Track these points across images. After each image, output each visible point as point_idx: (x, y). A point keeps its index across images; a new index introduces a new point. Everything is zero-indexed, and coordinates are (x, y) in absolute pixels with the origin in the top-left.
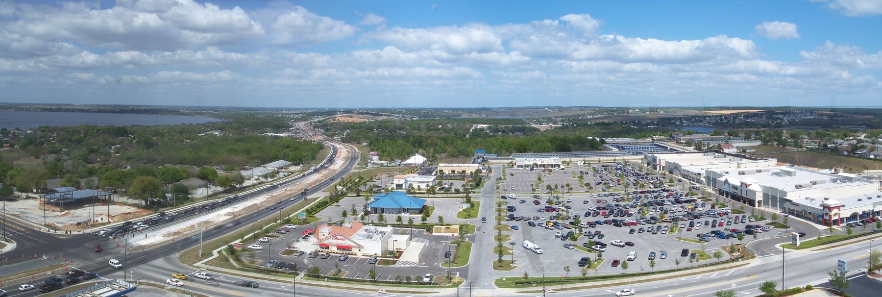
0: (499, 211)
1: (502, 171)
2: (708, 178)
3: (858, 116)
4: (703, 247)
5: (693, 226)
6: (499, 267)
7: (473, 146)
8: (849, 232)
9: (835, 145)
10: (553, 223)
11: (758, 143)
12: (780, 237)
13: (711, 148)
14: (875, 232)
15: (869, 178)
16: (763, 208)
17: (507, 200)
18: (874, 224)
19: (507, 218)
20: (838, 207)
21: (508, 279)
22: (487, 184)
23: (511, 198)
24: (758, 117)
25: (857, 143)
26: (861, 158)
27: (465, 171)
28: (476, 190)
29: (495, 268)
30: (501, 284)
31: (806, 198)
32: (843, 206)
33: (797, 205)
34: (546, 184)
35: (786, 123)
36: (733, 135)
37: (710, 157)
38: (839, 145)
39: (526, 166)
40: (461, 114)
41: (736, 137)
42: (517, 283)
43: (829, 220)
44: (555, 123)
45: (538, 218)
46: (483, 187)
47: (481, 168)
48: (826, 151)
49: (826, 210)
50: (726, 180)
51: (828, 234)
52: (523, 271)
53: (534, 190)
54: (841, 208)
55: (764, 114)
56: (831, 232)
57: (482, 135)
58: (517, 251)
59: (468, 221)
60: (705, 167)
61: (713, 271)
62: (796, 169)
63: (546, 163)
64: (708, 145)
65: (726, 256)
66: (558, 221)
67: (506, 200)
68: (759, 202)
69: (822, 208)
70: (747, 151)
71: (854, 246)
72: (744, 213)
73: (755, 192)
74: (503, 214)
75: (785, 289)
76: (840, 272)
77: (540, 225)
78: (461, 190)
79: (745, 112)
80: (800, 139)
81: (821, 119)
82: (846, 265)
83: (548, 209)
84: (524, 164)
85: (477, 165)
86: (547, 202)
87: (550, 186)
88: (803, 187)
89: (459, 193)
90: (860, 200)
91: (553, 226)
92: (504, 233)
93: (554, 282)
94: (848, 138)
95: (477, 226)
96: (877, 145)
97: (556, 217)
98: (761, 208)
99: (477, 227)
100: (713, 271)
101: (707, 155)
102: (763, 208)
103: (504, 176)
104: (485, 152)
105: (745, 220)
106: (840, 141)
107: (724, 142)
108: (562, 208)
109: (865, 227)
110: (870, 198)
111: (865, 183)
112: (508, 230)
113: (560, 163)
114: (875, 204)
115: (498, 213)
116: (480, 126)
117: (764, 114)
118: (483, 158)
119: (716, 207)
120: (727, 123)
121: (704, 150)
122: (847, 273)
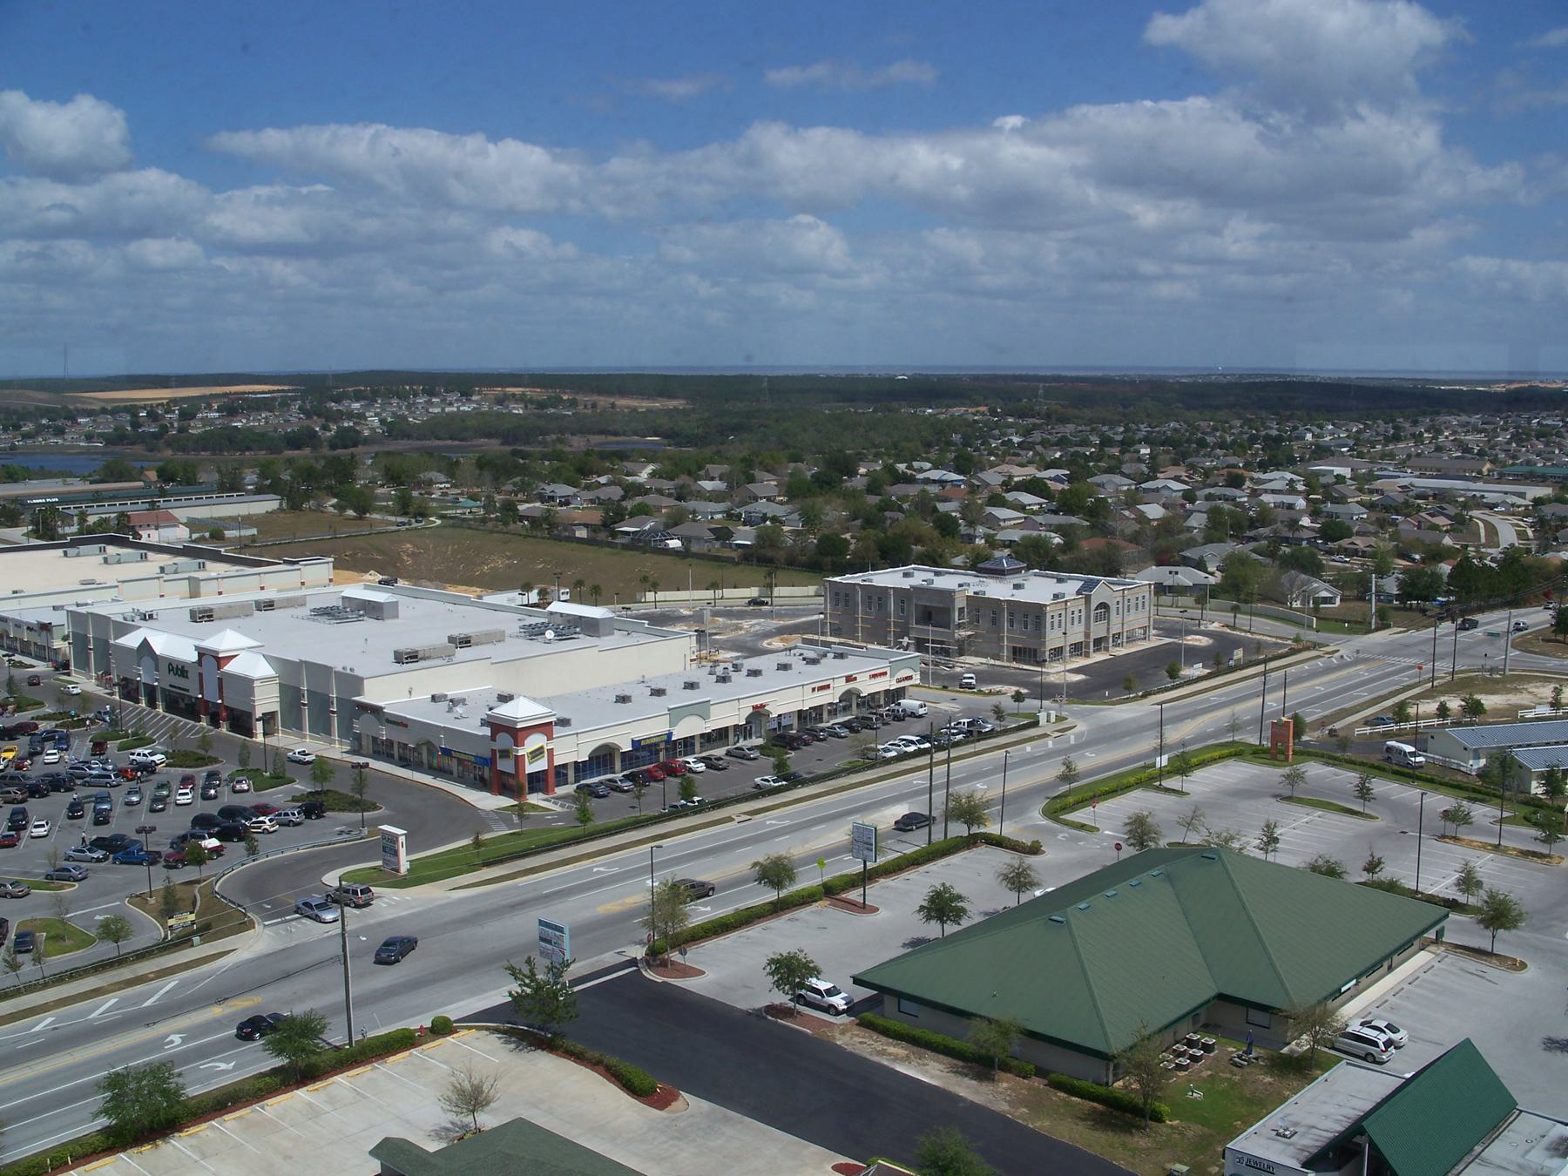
2: (80, 642)
4: (59, 902)
5: (24, 828)
11: (269, 504)
12: (340, 842)
13: (90, 530)
14: (677, 813)
15: (661, 621)
18: (674, 782)
20: (545, 728)
25: (624, 498)
26: (636, 548)
31: (434, 698)
32: (564, 722)
33: (400, 723)
35: (373, 429)
37: (88, 563)
38: (561, 504)
41: (189, 484)
43: (515, 776)
48: (512, 526)
49: (504, 740)
50: (145, 643)
51: (510, 825)
54: (558, 732)
56: (521, 817)
60: (69, 601)
61: (97, 992)
62: (403, 592)
64: (83, 517)
65: (151, 929)
68: (268, 718)
69: (487, 731)
70: (229, 534)
71: (599, 867)
72: (216, 760)
73: (252, 681)
75: (357, 1037)
76: (547, 962)
79: (225, 395)
80: (418, 485)
81: (499, 415)
82: (566, 937)
88: (423, 659)
90: (623, 699)
94: (595, 478)
96: (692, 504)
98: (271, 741)
100: (97, 992)
101: (78, 555)
102: (283, 740)
105: (215, 787)
106: (563, 490)
107: (141, 505)
109: (638, 797)
110: (658, 692)
114: (676, 714)
117: (294, 399)
119: (112, 745)
121: (64, 536)
122: (568, 966)
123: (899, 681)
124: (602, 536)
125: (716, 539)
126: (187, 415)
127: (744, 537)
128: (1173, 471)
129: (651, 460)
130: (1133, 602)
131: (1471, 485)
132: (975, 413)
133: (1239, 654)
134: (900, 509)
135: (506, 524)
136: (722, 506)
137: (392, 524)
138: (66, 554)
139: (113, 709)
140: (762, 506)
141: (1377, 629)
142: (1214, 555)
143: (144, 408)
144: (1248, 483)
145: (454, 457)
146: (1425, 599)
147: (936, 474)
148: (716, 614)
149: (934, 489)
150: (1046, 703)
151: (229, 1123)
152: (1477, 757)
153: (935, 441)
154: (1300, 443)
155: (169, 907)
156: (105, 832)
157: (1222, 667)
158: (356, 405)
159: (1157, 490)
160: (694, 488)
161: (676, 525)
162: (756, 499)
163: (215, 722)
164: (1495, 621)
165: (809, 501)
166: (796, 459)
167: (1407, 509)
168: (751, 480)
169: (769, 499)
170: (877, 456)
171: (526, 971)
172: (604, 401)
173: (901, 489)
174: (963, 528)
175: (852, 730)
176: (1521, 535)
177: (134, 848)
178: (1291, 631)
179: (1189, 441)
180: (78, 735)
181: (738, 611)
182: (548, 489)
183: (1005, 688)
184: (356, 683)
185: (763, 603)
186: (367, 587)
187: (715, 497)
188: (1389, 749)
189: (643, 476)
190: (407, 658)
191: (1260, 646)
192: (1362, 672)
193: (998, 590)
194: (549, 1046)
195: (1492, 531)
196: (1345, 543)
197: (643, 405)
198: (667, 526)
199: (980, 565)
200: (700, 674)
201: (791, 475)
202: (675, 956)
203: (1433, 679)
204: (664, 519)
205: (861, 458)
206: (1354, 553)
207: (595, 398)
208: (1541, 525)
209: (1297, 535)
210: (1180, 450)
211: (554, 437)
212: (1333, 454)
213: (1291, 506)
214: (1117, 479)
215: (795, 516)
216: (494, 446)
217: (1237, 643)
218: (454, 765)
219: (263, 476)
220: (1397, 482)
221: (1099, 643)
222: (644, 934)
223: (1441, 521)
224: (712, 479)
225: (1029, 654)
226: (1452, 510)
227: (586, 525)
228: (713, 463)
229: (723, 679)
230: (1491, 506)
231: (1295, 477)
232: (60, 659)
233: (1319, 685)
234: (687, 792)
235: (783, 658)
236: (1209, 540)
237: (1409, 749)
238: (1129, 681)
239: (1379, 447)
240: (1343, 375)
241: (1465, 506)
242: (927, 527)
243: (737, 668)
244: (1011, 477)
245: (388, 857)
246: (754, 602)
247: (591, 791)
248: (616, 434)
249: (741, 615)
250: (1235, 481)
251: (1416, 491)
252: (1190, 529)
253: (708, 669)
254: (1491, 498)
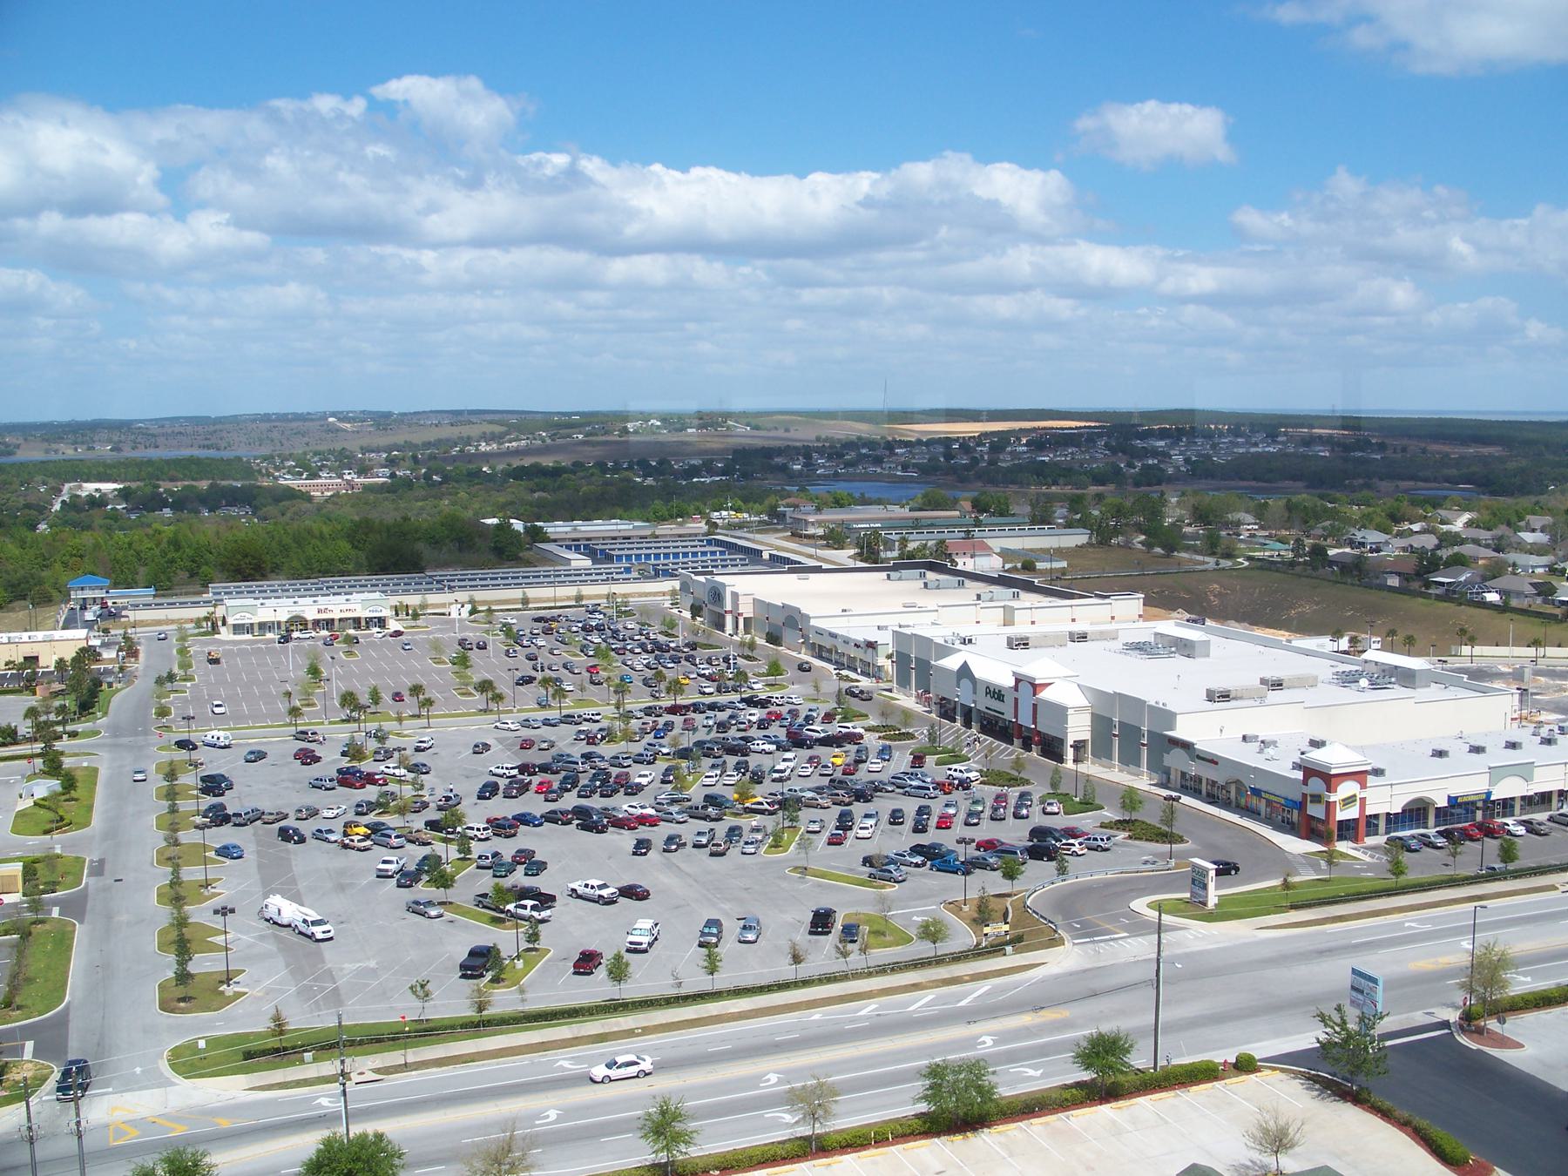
0: (171, 794)
1: (175, 652)
2: (901, 660)
3: (1446, 449)
4: (882, 900)
5: (850, 828)
6: (183, 1000)
7: (65, 565)
8: (1397, 869)
9: (1356, 552)
10: (366, 826)
11: (1078, 538)
12: (1147, 872)
13: (911, 556)
14: (1493, 876)
15: (1479, 677)
16: (1090, 768)
17: (200, 755)
18: (1492, 844)
19: (199, 820)
20: (1359, 776)
21: (214, 1043)
22: (121, 701)
23: (214, 746)
24: (1078, 446)
25: (1438, 547)
26: (1451, 600)
27: (36, 658)
28: (79, 727)
29: (165, 1006)
30: (190, 1063)
32: (1378, 772)
33: (1212, 761)
34: (337, 687)
35: (1177, 468)
36: (990, 509)
37: (908, 587)
38: (1371, 551)
39: (264, 627)
40: (18, 446)
41: (1001, 515)
42: (248, 1055)
43: (1326, 822)
44: (363, 471)
45: (313, 813)
46: (105, 714)
47: (96, 642)
48: (1321, 571)
49: (1316, 785)
51: (1318, 870)
52: (268, 1009)
53: (294, 712)
54: (1371, 780)
55: (1100, 435)
56: (1330, 863)
57: (98, 521)
58: (242, 935)
59: (58, 843)
60: (892, 622)
61: (916, 987)
62: (1210, 631)
63: (337, 615)
64: (904, 542)
65: (963, 936)
66: (384, 819)
67: (195, 755)
68: (1079, 746)
69: (1299, 775)
70: (1039, 565)
72: (1027, 782)
73: (1065, 709)
74: (185, 805)
75: (1162, 1063)
76: (1357, 1012)
77: (320, 835)
78: (25, 728)
79: (1034, 430)
80: (1226, 525)
81: (1305, 457)
82: (1380, 988)
83: (347, 778)
84: (256, 620)
85: (82, 633)
86: (344, 754)
87: (351, 694)
88: (1235, 699)
89: (15, 743)
90: (1440, 754)
91: (367, 837)
92: (192, 873)
93: (379, 1041)
94: (1406, 526)
95: (90, 857)
96: (1512, 557)
97: (378, 805)
99: (92, 861)
100: (916, 987)
101: (900, 579)
102: (1090, 768)
103: (185, 666)
104: (107, 582)
105: (1027, 807)
106: (1373, 537)
107: (958, 533)
108: (397, 772)
109: (1454, 855)
110: (1477, 750)
112: (205, 861)
113: (387, 613)
114: (1496, 773)
115: (166, 803)
116: (89, 488)
117: (1100, 435)
118: (104, 606)
119: (930, 760)
120: (966, 468)
122: (1381, 1018)
125: (1538, 595)
136: (1545, 560)
138: (889, 577)
151: (1036, 1126)
155: (982, 916)
156: (923, 839)
158: (1162, 443)
160: (1513, 540)
161: (1495, 577)
171: (1336, 1018)
177: (951, 857)
180: (899, 748)
181: (1562, 672)
187: (1537, 550)
194: (1356, 1098)
200: (1523, 735)
202: (1492, 1024)
211: (1361, 481)
218: (1262, 806)
222: (1459, 997)
224: (1533, 531)
227: (1399, 574)
228: (1534, 514)
229: (1548, 741)
234: (1507, 854)
245: (1196, 889)
247: (1402, 844)
253: (1532, 730)
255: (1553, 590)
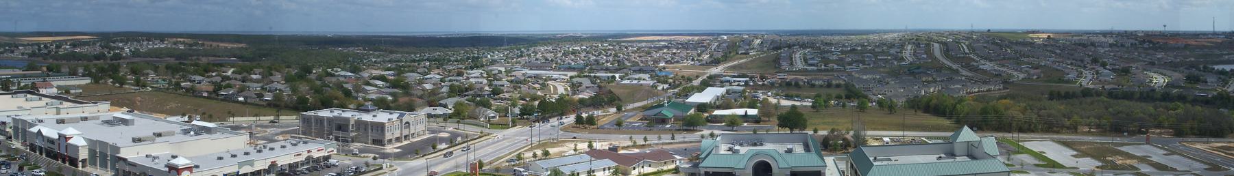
2: (16, 129)
3: (227, 45)
11: (87, 81)
15: (236, 128)
16: (88, 169)
25: (222, 81)
31: (147, 156)
32: (197, 167)
33: (134, 165)
36: (54, 71)
37: (20, 101)
38: (197, 83)
48: (178, 91)
50: (39, 131)
54: (194, 170)
55: (98, 41)
60: (13, 114)
68: (84, 161)
69: (167, 169)
70: (72, 91)
79: (73, 40)
80: (143, 75)
81: (174, 49)
88: (144, 141)
90: (220, 158)
94: (211, 74)
98: (84, 170)
101: (17, 97)
102: (88, 169)
106: (198, 78)
107: (40, 79)
110: (234, 156)
111: (229, 135)
114: (241, 165)
117: (98, 41)
119: (26, 168)
121: (12, 90)
123: (328, 152)
124: (213, 95)
126: (58, 47)
127: (268, 97)
128: (437, 71)
129: (232, 67)
130: (419, 121)
131: (548, 72)
132: (358, 50)
133: (459, 139)
134: (329, 86)
135: (176, 90)
136: (260, 85)
137: (133, 89)
139: (27, 155)
140: (275, 85)
141: (512, 127)
142: (451, 102)
143: (43, 44)
144: (465, 74)
145: (157, 65)
146: (530, 115)
147: (343, 73)
148: (257, 126)
149: (342, 79)
150: (386, 160)
152: (547, 170)
153: (343, 62)
154: (486, 59)
157: (453, 144)
159: (431, 78)
161: (242, 91)
162: (273, 82)
163: (64, 162)
164: (554, 121)
165: (294, 83)
166: (289, 67)
167: (524, 82)
168: (271, 75)
169: (278, 82)
170: (320, 66)
172: (215, 44)
173: (328, 79)
174: (354, 94)
175: (310, 171)
176: (566, 90)
178: (479, 129)
179: (444, 60)
180: (14, 163)
182: (193, 77)
183: (370, 155)
184: (117, 149)
185: (275, 122)
186: (123, 113)
187: (257, 81)
188: (515, 170)
189: (229, 73)
190: (137, 140)
191: (467, 136)
192: (506, 143)
193: (367, 117)
195: (555, 88)
196: (501, 95)
197: (230, 46)
198: (238, 92)
199: (361, 108)
200: (250, 149)
201: (287, 73)
203: (532, 144)
204: (237, 90)
205: (313, 67)
206: (502, 99)
207: (211, 43)
208: (573, 85)
209: (483, 93)
210: (439, 63)
211: (195, 57)
212: (498, 62)
213: (481, 83)
214: (415, 75)
215: (288, 89)
216: (172, 61)
217: (459, 135)
219: (85, 70)
220: (520, 73)
221: (406, 137)
223: (537, 86)
224: (256, 74)
225: (379, 142)
226: (541, 82)
227: (207, 92)
229: (260, 151)
230: (555, 80)
231: (483, 72)
232: (8, 135)
233: (490, 149)
235: (283, 143)
236: (449, 97)
237: (522, 170)
238: (417, 151)
239: (515, 60)
240: (503, 33)
241: (546, 80)
242: (340, 94)
243: (265, 147)
244: (372, 74)
246: (272, 122)
248: (219, 57)
249: (266, 127)
250: (460, 74)
251: (528, 75)
252: (443, 93)
254: (555, 76)
255: (263, 96)
